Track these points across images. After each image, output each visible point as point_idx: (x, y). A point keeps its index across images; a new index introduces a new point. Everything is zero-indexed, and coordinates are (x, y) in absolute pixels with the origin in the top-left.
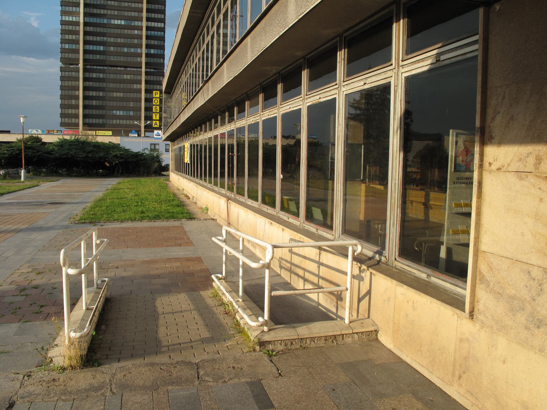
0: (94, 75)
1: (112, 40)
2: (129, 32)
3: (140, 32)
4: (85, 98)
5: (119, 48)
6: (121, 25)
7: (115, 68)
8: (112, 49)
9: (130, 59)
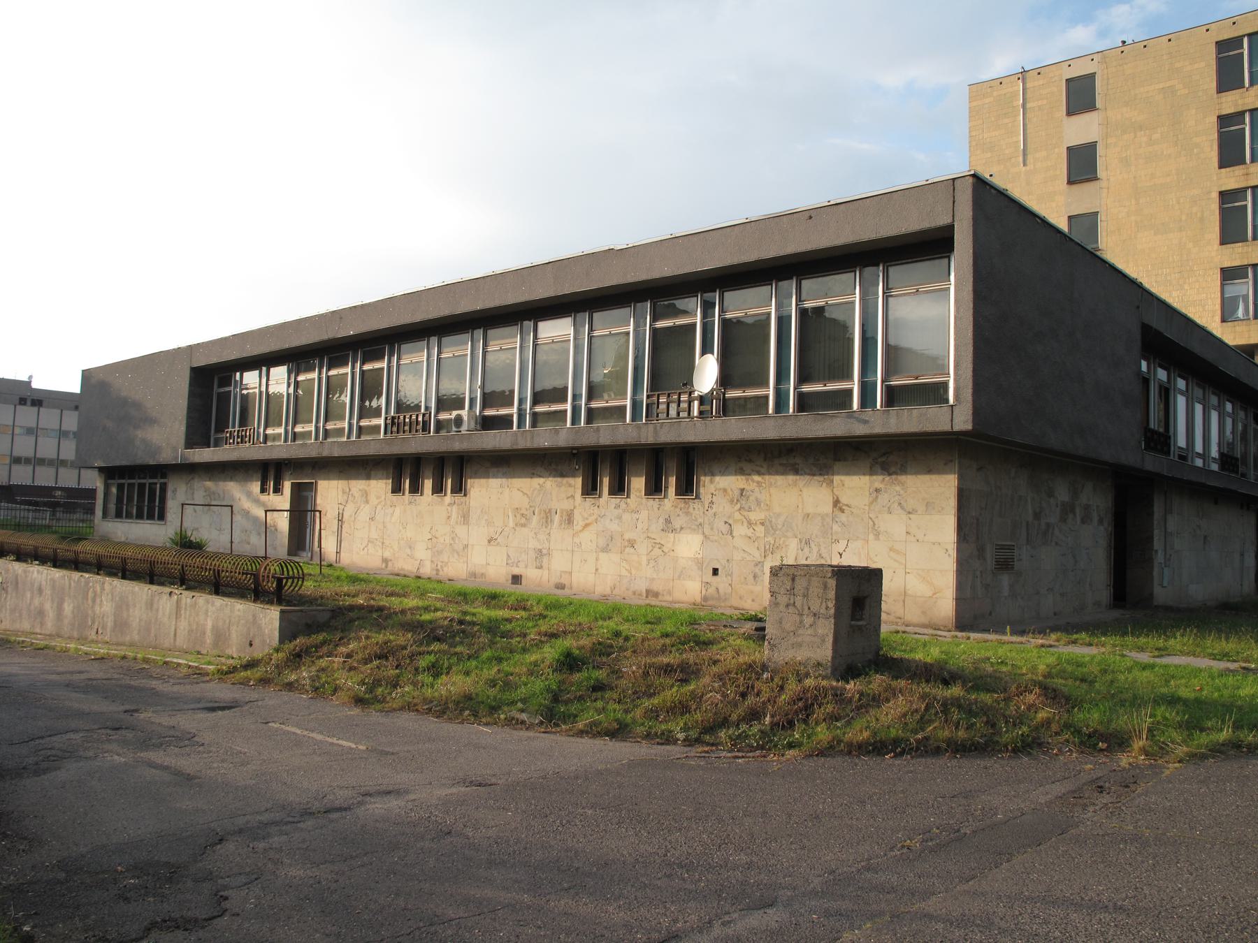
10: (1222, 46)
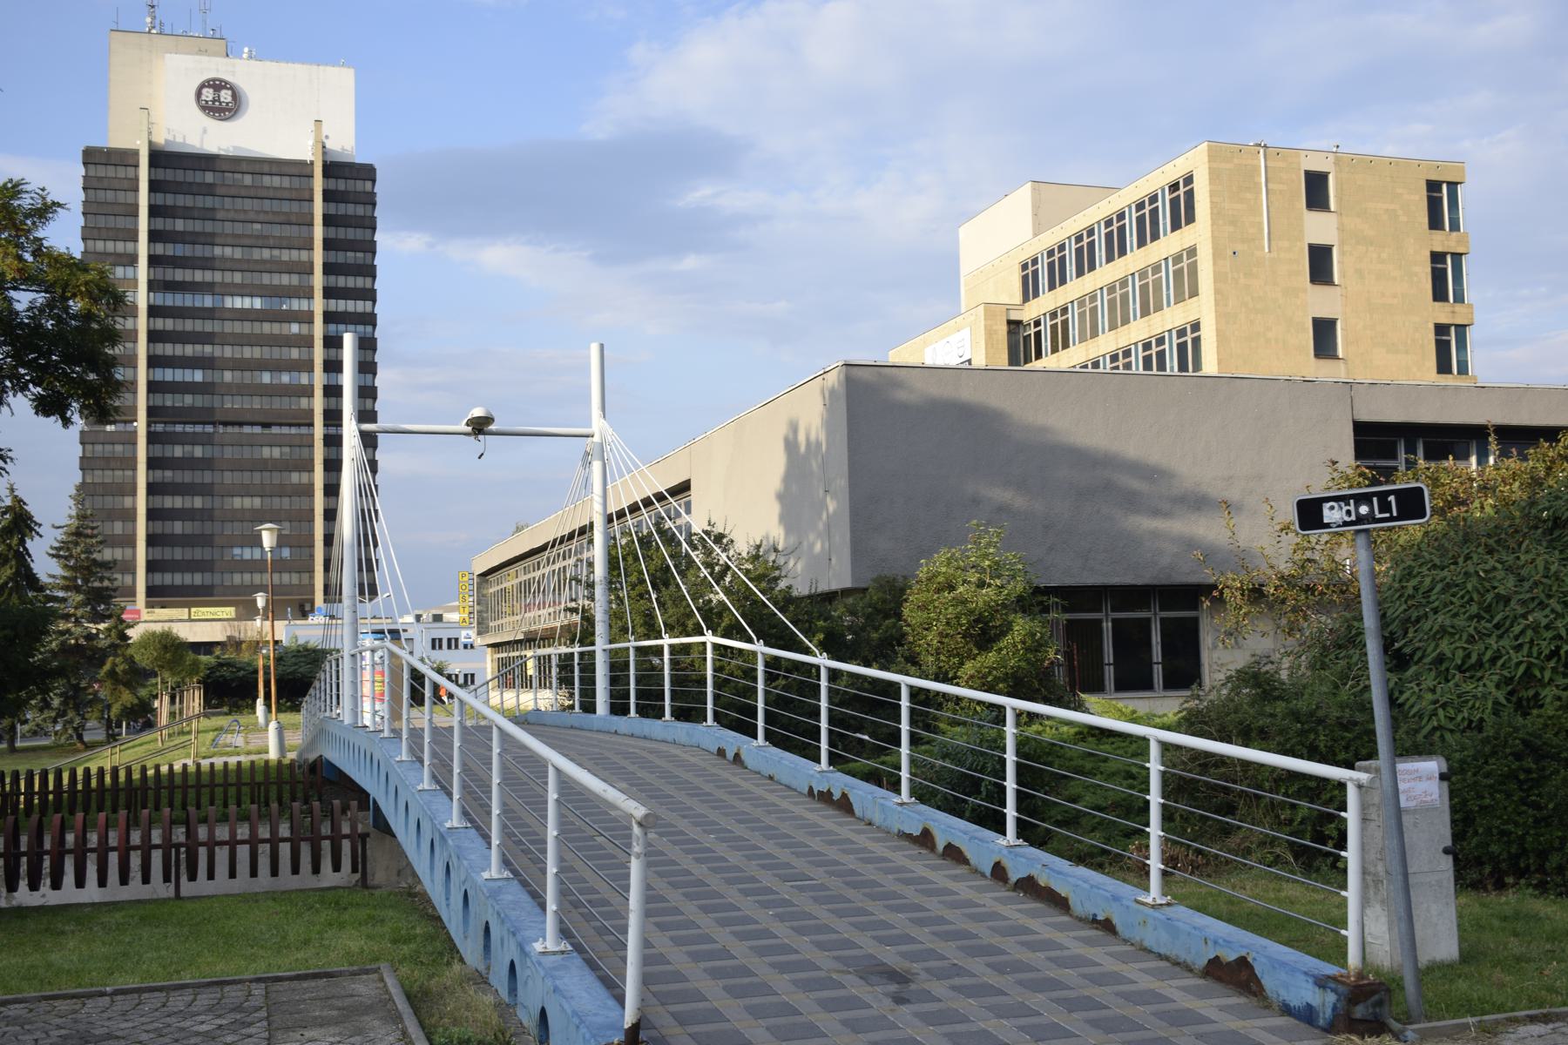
0: (178, 451)
1: (228, 352)
2: (276, 328)
3: (305, 329)
4: (152, 514)
5: (247, 374)
6: (252, 310)
7: (236, 429)
8: (228, 376)
9: (278, 403)
10: (1433, 186)
